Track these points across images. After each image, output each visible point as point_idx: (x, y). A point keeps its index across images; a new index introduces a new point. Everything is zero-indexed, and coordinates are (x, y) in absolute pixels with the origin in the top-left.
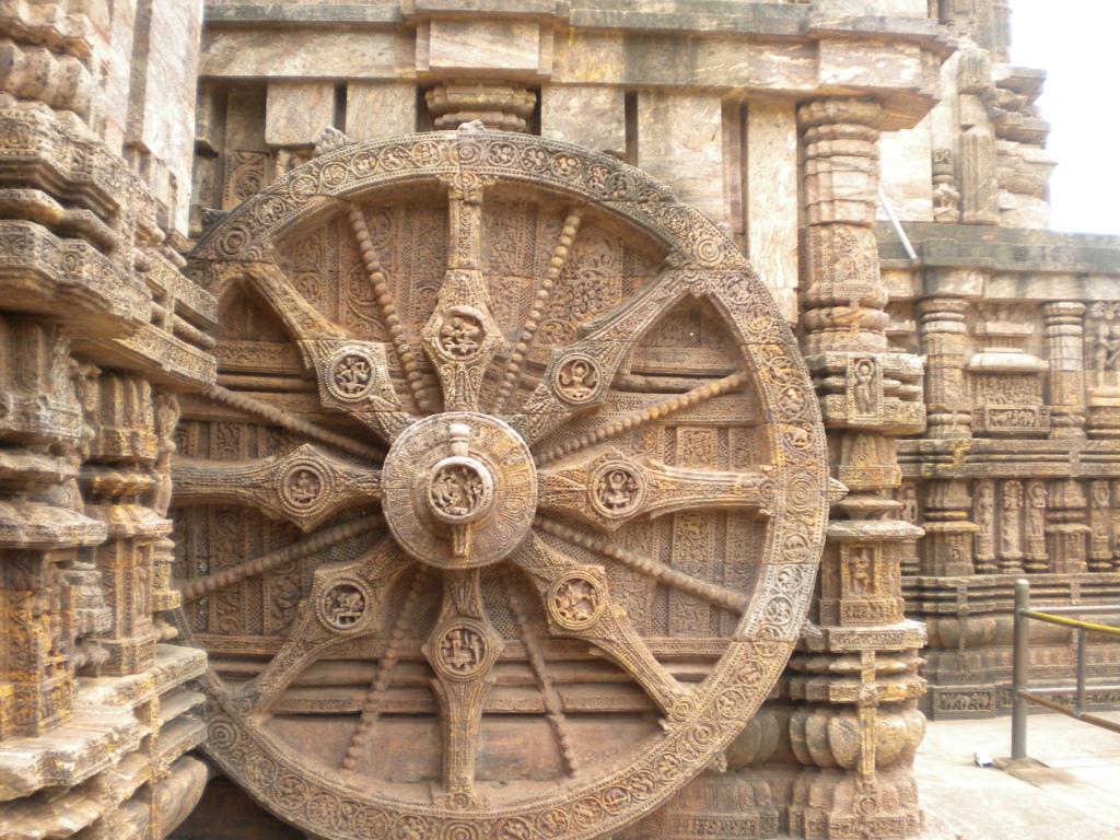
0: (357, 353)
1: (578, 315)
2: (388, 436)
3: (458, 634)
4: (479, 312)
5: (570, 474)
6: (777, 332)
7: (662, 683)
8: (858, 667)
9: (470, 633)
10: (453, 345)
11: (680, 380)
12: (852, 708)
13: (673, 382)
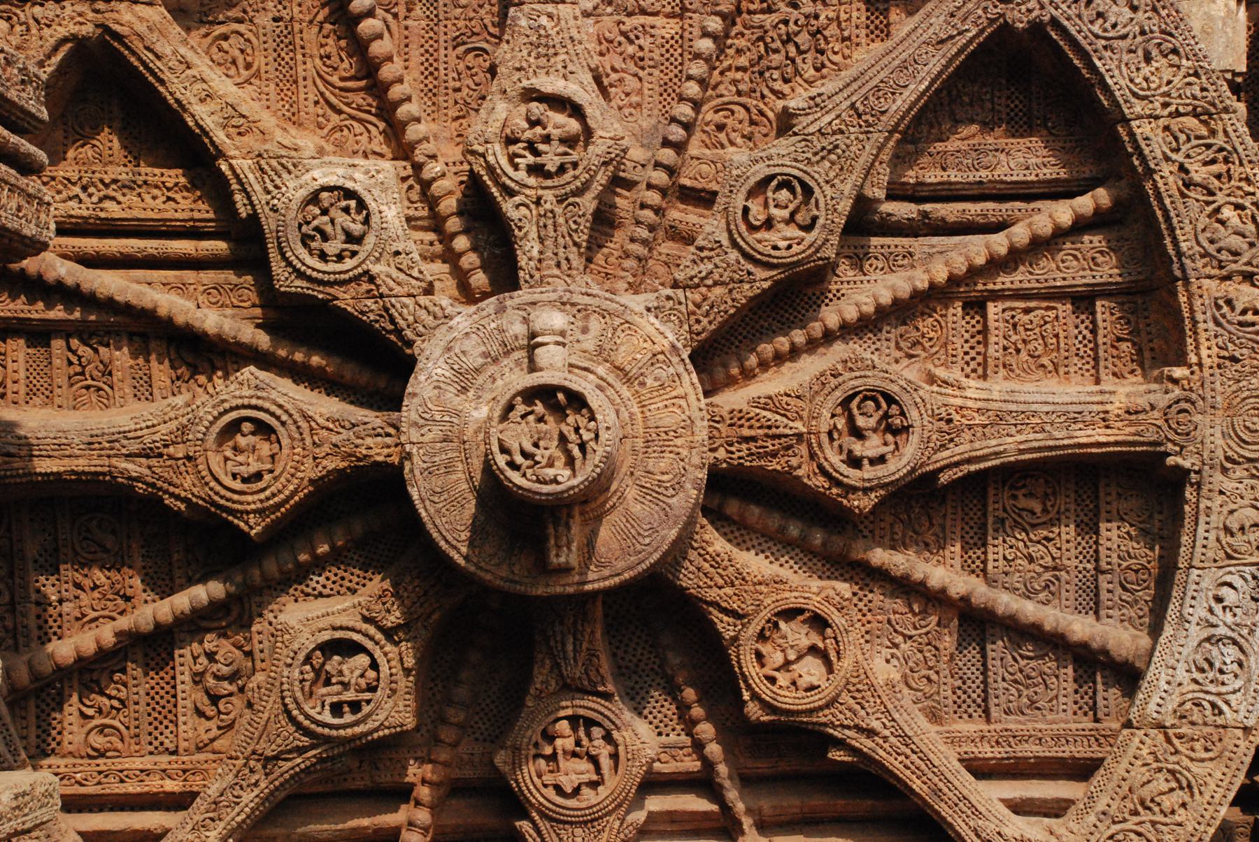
0: (339, 184)
1: (778, 85)
2: (410, 344)
3: (565, 723)
4: (579, 89)
5: (769, 403)
6: (1196, 90)
7: (977, 813)
9: (590, 723)
10: (531, 159)
11: (990, 205)
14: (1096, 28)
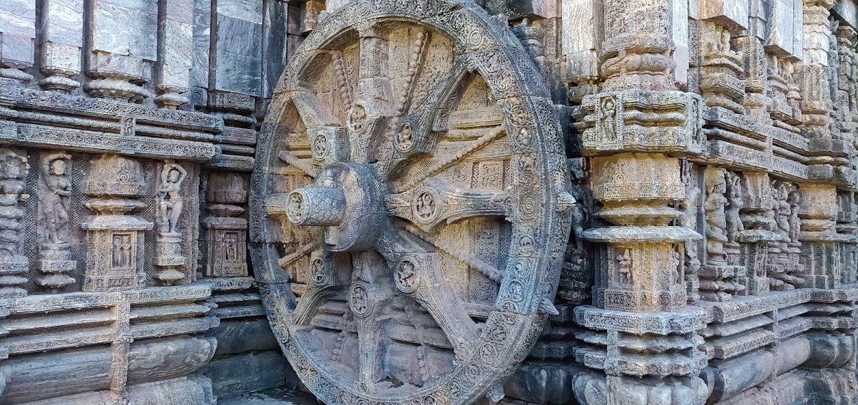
8: (605, 343)
12: (601, 373)
13: (474, 132)
14: (489, 70)
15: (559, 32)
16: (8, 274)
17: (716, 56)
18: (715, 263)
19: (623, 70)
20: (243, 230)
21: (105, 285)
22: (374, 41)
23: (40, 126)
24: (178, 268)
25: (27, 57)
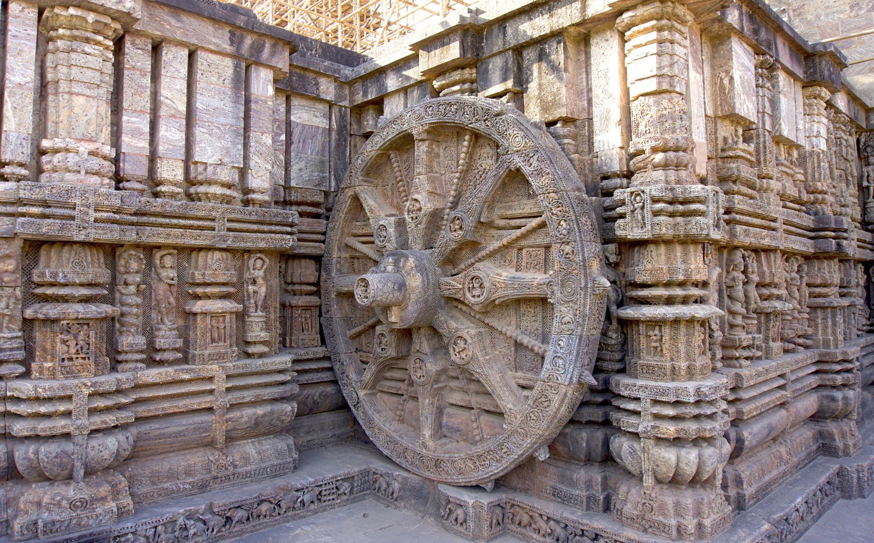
12: (636, 436)
13: (518, 222)
15: (591, 133)
16: (131, 352)
17: (731, 149)
18: (736, 333)
19: (650, 166)
20: (316, 307)
21: (206, 360)
22: (427, 143)
23: (153, 228)
24: (264, 343)
25: (142, 171)
